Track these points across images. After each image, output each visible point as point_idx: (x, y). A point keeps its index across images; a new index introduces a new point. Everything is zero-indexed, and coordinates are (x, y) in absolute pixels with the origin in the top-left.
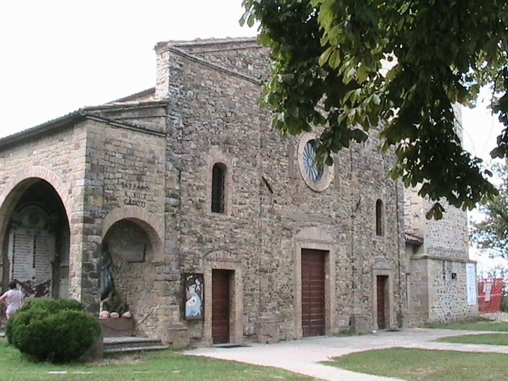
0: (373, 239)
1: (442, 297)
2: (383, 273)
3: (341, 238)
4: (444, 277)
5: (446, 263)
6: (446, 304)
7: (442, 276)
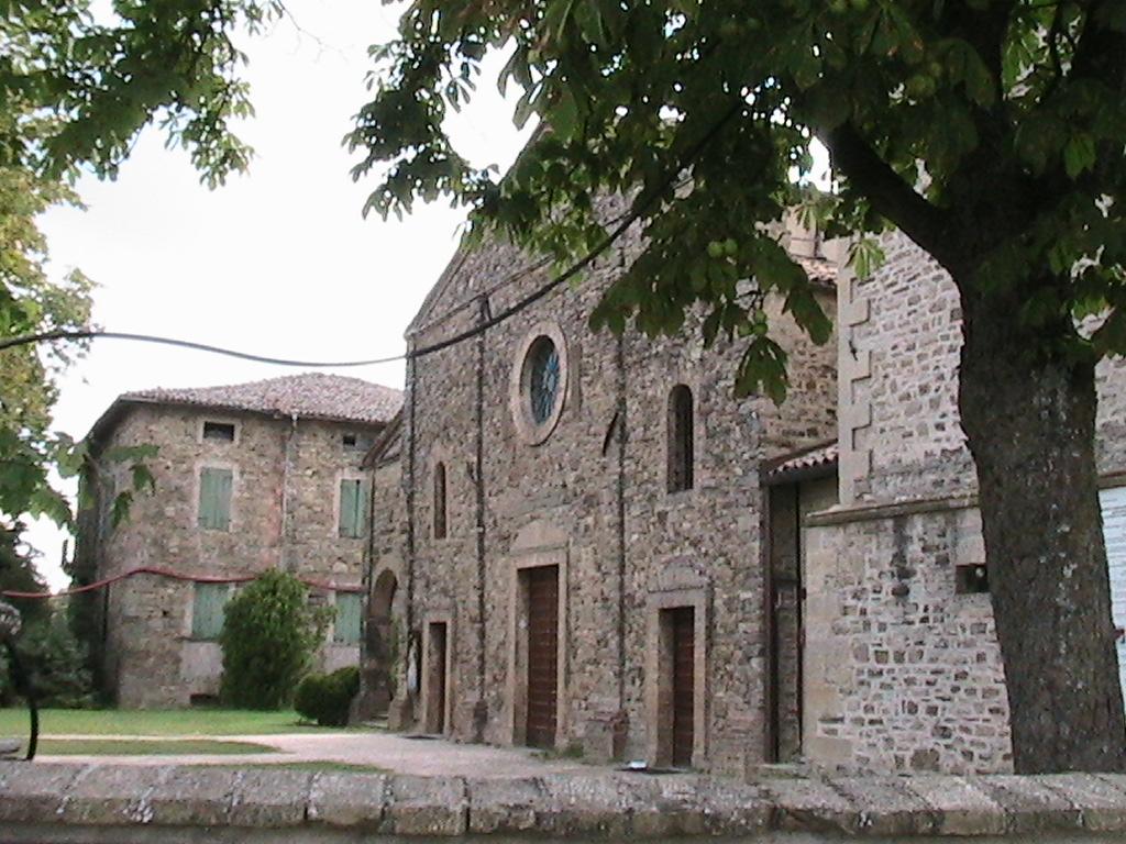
0: (659, 508)
1: (886, 678)
2: (677, 600)
3: (582, 528)
4: (901, 593)
5: (917, 527)
6: (913, 709)
7: (889, 584)
